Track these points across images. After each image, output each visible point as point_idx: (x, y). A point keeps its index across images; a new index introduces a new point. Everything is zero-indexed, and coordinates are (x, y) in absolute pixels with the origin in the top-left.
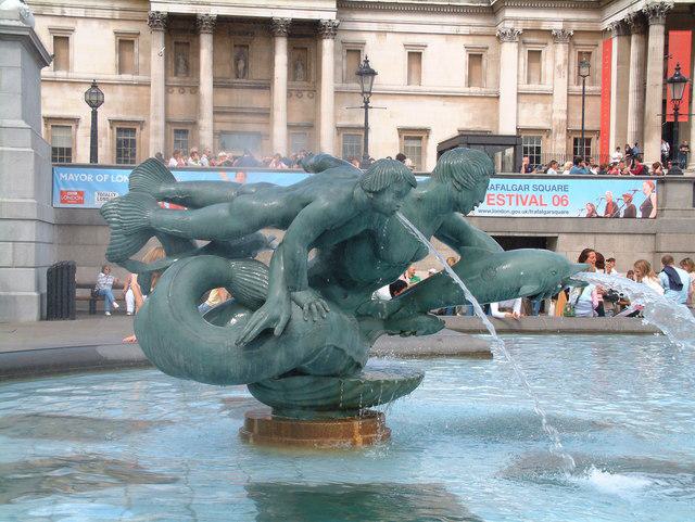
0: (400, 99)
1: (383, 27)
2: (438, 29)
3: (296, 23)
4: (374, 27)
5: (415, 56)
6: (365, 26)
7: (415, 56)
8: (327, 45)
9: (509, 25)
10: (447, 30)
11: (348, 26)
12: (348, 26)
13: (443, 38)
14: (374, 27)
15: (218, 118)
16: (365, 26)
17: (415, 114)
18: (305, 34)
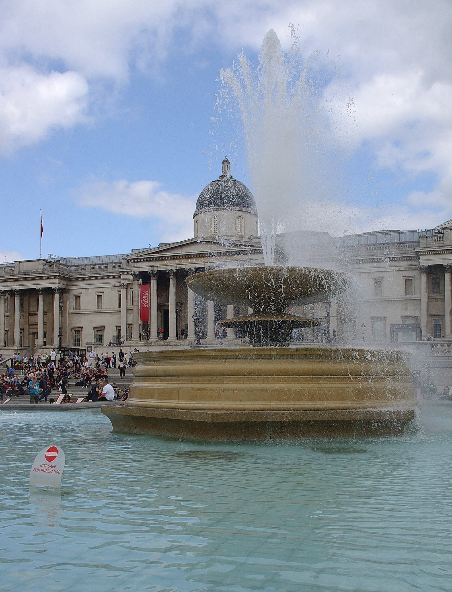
0: (94, 315)
1: (88, 287)
2: (107, 285)
3: (44, 289)
4: (84, 287)
5: (99, 297)
6: (81, 287)
7: (99, 297)
8: (57, 296)
9: (123, 282)
10: (111, 285)
11: (75, 287)
12: (75, 287)
13: (109, 289)
14: (84, 287)
15: (31, 327)
16: (81, 287)
17: (99, 321)
18: (49, 292)
